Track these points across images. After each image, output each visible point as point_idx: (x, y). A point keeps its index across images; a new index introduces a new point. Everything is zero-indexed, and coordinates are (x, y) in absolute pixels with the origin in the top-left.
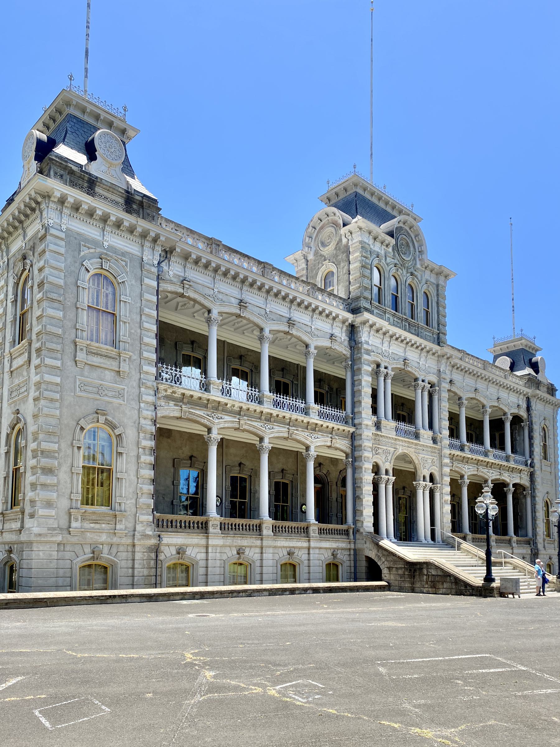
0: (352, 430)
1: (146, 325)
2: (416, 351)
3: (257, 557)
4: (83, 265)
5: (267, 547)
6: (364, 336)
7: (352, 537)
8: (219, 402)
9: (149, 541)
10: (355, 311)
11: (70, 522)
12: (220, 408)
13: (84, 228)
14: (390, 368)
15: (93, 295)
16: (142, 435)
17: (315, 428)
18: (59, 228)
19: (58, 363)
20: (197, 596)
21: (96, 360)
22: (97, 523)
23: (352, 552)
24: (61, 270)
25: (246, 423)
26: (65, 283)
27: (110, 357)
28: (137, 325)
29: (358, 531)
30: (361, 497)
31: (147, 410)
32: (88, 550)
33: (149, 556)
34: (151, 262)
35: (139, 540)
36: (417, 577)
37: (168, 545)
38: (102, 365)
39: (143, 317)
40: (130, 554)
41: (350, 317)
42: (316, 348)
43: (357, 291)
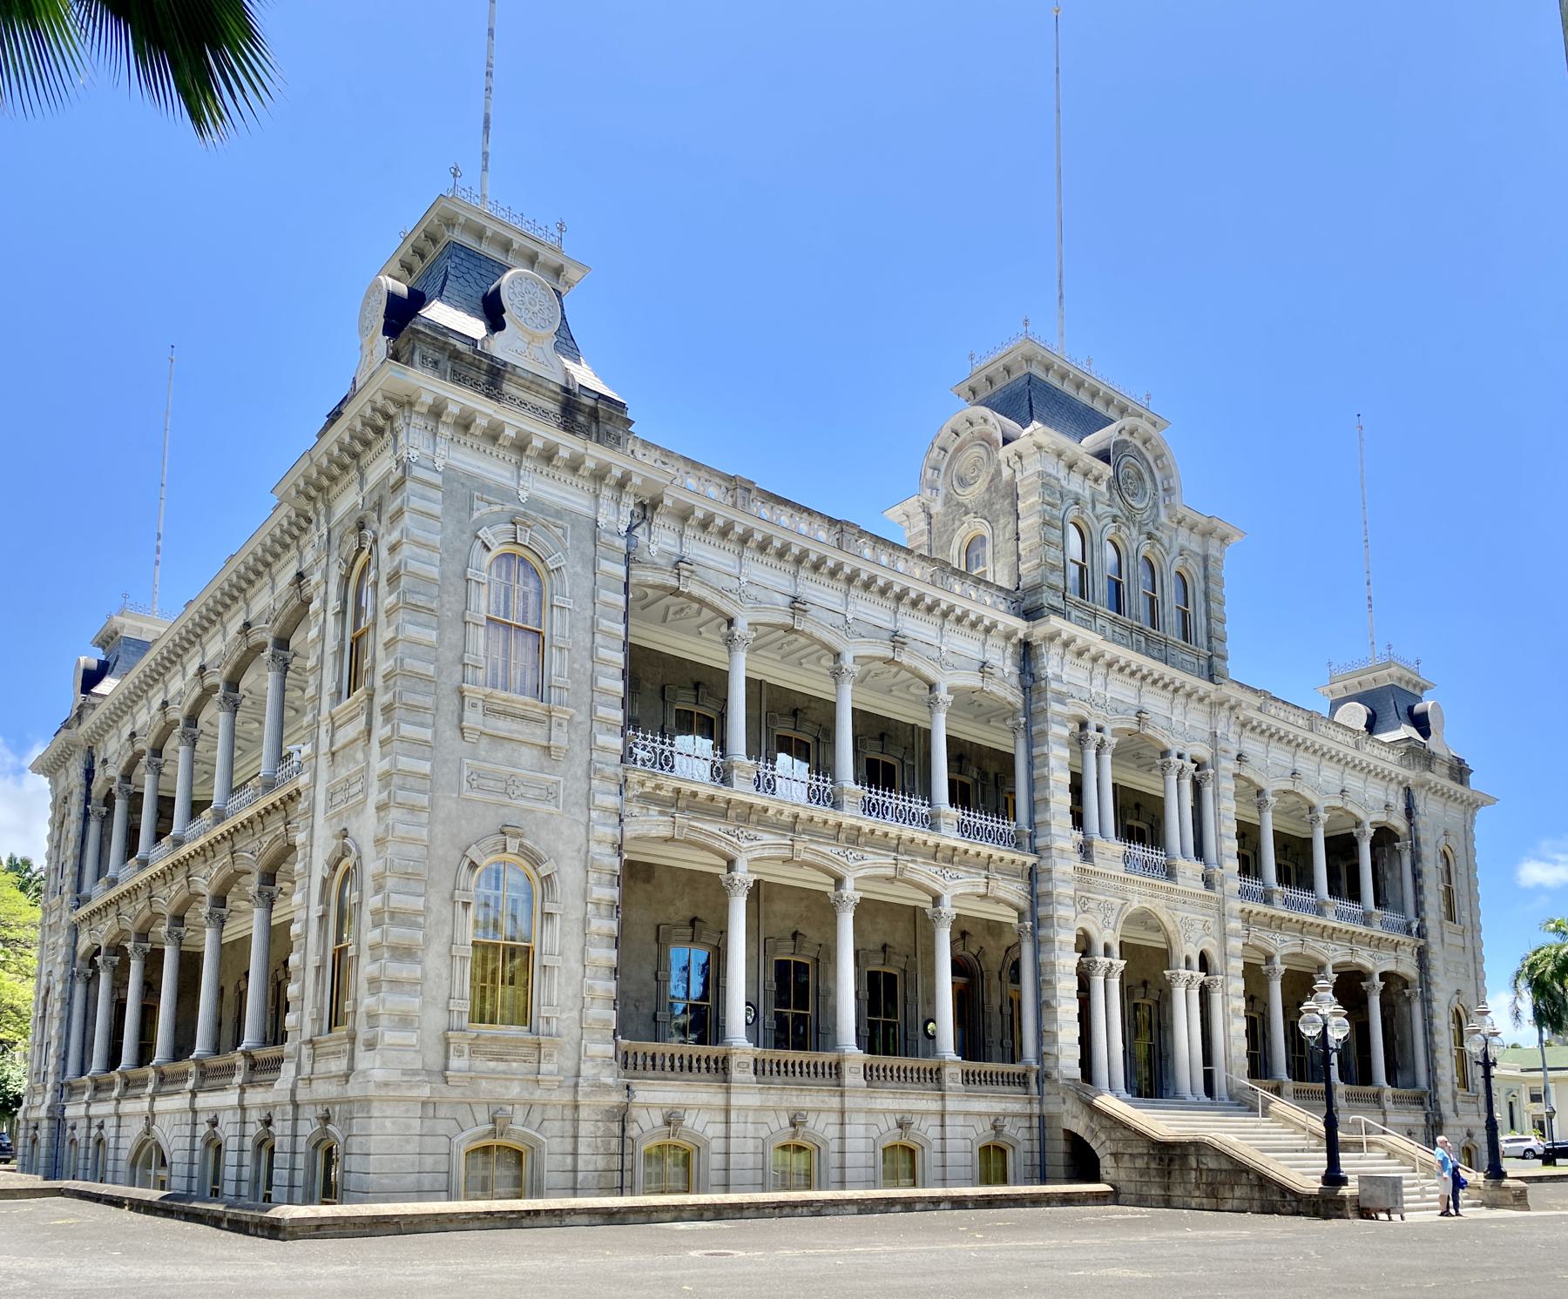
0: (1031, 860)
1: (603, 653)
2: (1164, 693)
3: (832, 1132)
4: (477, 537)
5: (852, 1111)
6: (1051, 663)
7: (1034, 1089)
8: (751, 806)
9: (607, 1098)
10: (1031, 614)
11: (447, 1058)
12: (754, 818)
13: (482, 465)
14: (1108, 729)
15: (497, 596)
16: (593, 876)
17: (951, 857)
18: (430, 465)
19: (427, 734)
20: (707, 1214)
21: (503, 726)
22: (502, 1060)
23: (1035, 1122)
24: (434, 549)
25: (806, 848)
26: (442, 574)
28: (586, 654)
29: (1047, 1076)
30: (1054, 1003)
31: (605, 824)
32: (482, 1115)
33: (609, 1129)
34: (614, 529)
35: (586, 1095)
36: (1176, 1175)
37: (647, 1107)
38: (515, 736)
39: (598, 637)
40: (568, 1124)
41: (1021, 626)
42: (950, 691)
43: (1034, 573)
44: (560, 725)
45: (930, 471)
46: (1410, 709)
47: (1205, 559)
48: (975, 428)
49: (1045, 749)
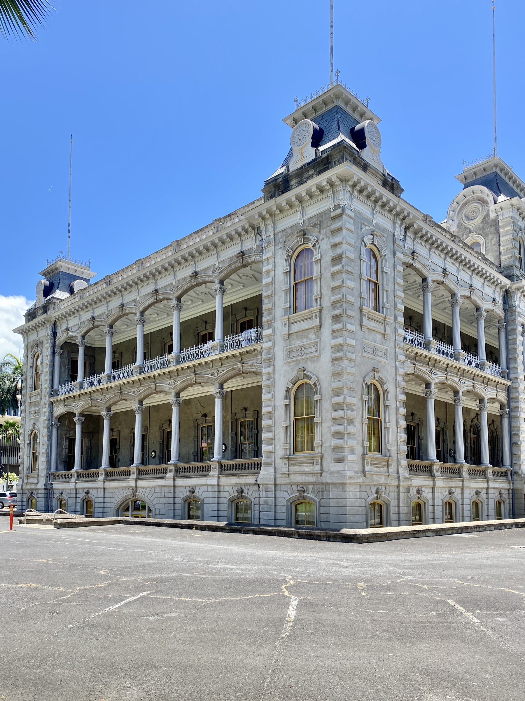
4: (363, 241)
23: (511, 491)
27: (379, 322)
29: (516, 473)
30: (519, 443)
38: (376, 329)
44: (388, 324)
45: (451, 213)
48: (475, 195)
49: (515, 337)
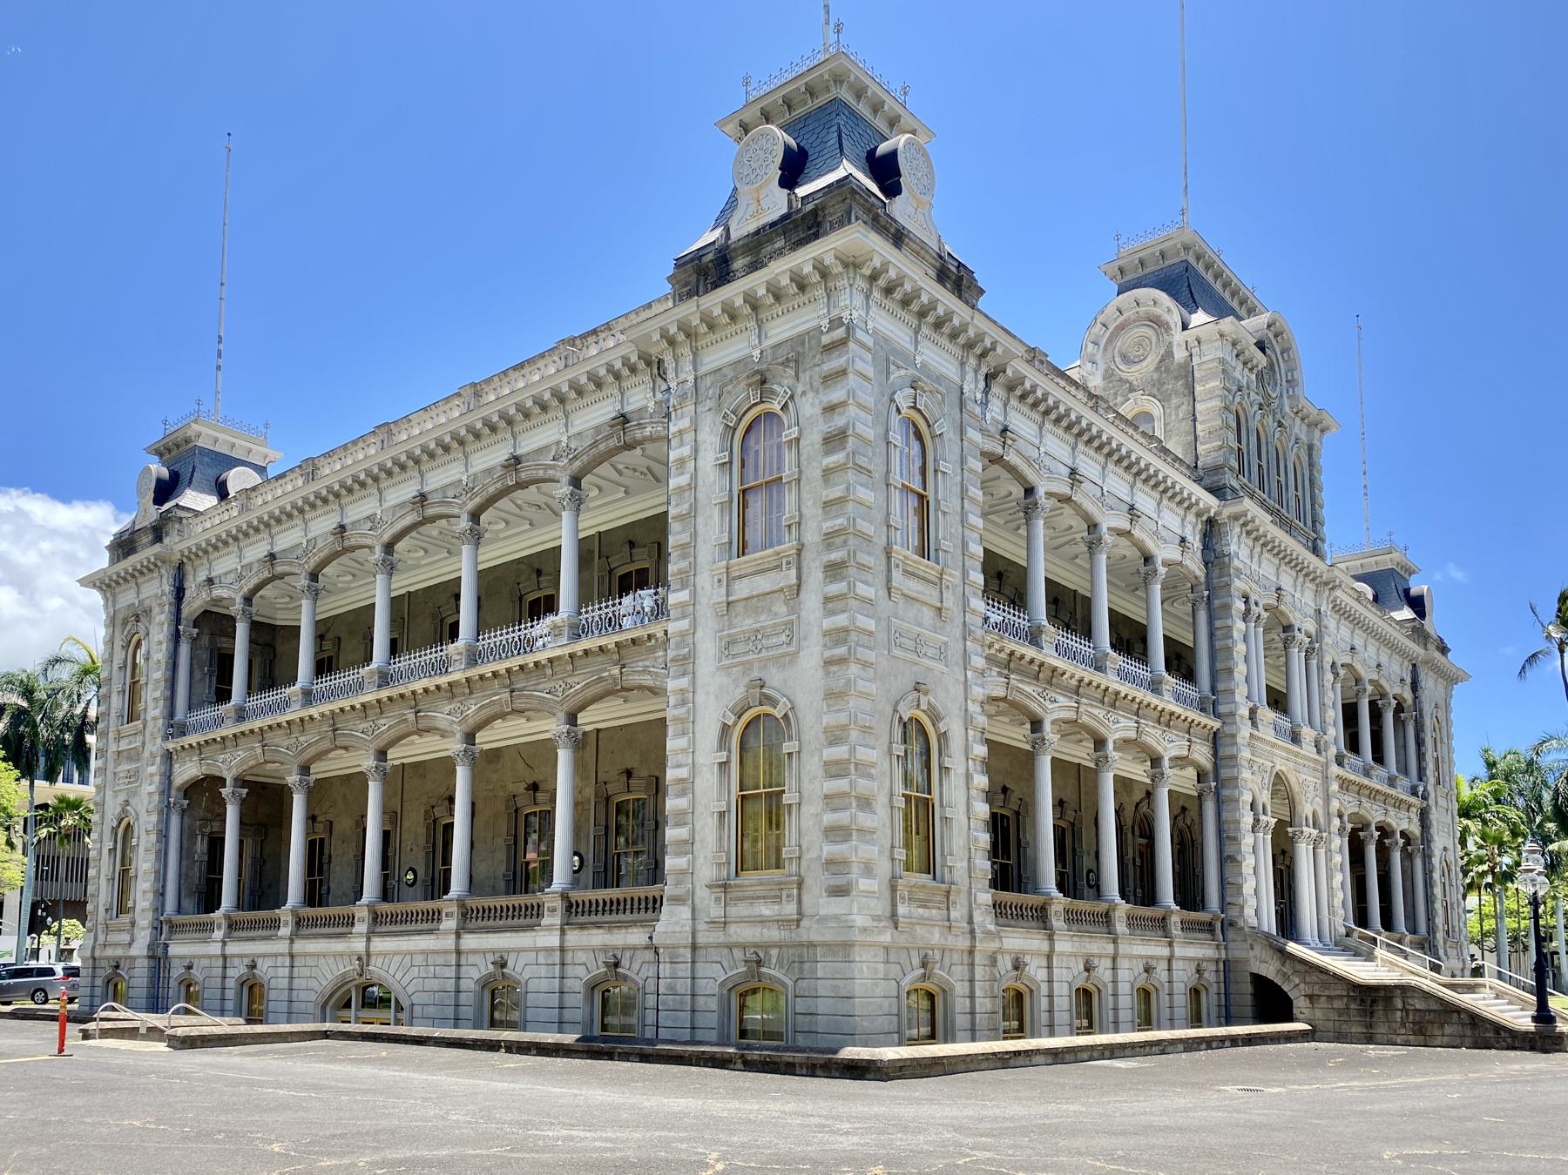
0: (1216, 725)
4: (892, 400)
10: (1217, 491)
11: (894, 906)
29: (1232, 924)
36: (1379, 1014)
38: (921, 597)
45: (1090, 346)
46: (1407, 591)
47: (1310, 448)
48: (1142, 309)
49: (1229, 622)
